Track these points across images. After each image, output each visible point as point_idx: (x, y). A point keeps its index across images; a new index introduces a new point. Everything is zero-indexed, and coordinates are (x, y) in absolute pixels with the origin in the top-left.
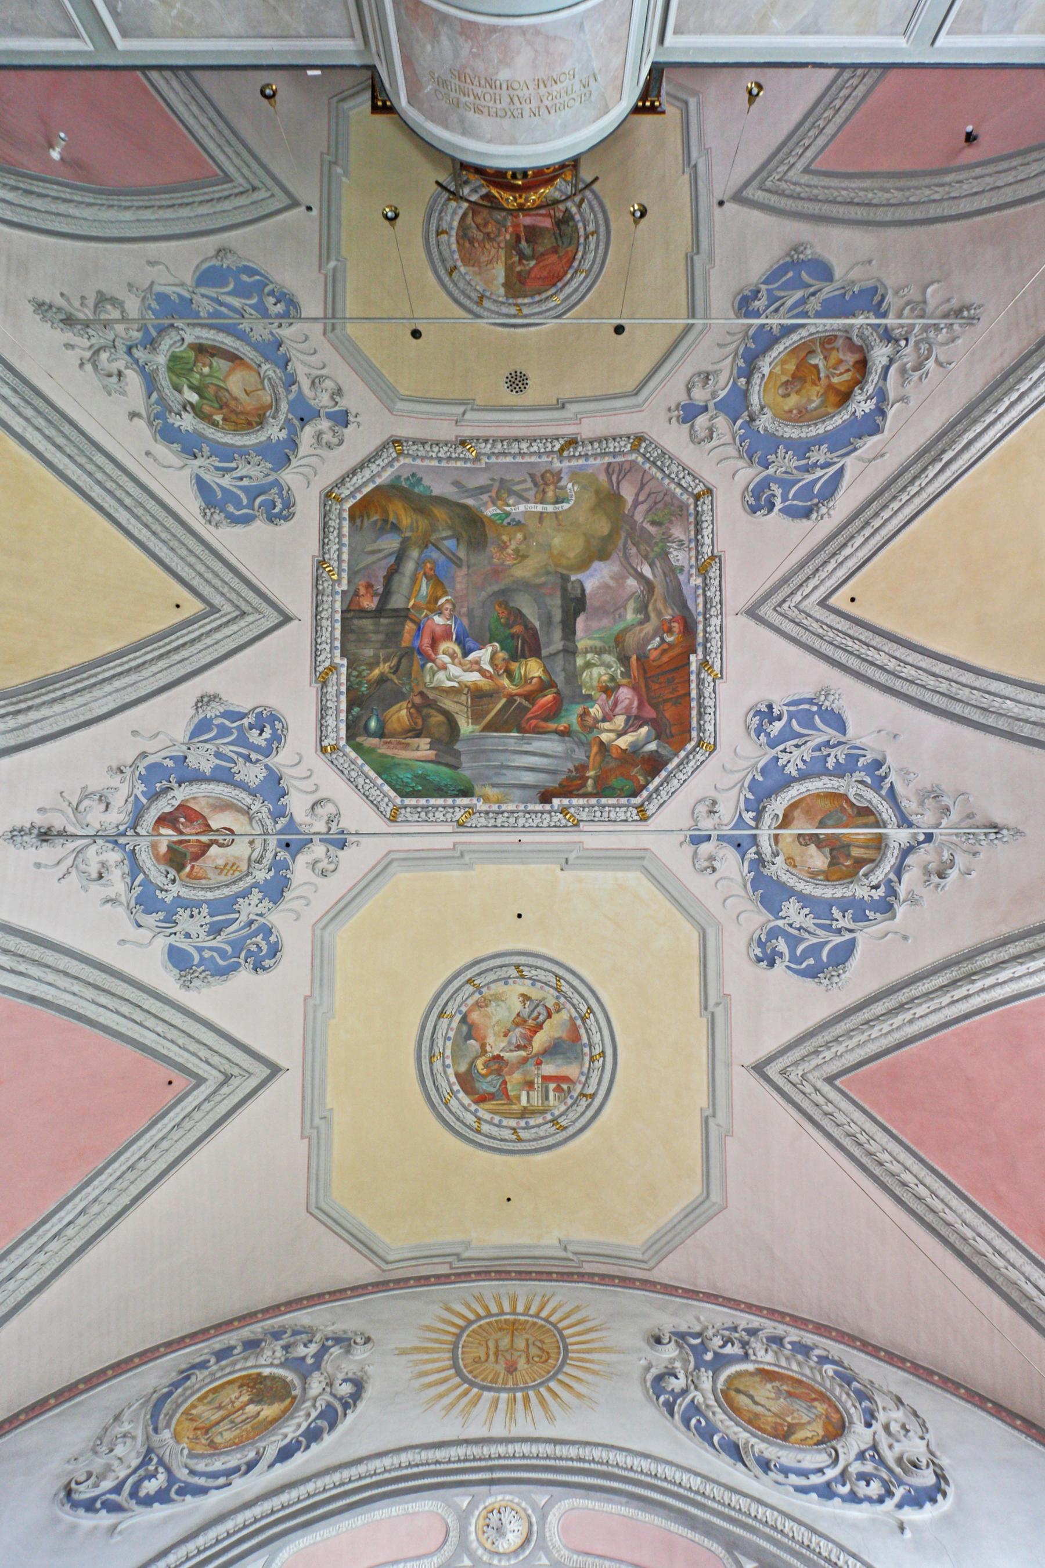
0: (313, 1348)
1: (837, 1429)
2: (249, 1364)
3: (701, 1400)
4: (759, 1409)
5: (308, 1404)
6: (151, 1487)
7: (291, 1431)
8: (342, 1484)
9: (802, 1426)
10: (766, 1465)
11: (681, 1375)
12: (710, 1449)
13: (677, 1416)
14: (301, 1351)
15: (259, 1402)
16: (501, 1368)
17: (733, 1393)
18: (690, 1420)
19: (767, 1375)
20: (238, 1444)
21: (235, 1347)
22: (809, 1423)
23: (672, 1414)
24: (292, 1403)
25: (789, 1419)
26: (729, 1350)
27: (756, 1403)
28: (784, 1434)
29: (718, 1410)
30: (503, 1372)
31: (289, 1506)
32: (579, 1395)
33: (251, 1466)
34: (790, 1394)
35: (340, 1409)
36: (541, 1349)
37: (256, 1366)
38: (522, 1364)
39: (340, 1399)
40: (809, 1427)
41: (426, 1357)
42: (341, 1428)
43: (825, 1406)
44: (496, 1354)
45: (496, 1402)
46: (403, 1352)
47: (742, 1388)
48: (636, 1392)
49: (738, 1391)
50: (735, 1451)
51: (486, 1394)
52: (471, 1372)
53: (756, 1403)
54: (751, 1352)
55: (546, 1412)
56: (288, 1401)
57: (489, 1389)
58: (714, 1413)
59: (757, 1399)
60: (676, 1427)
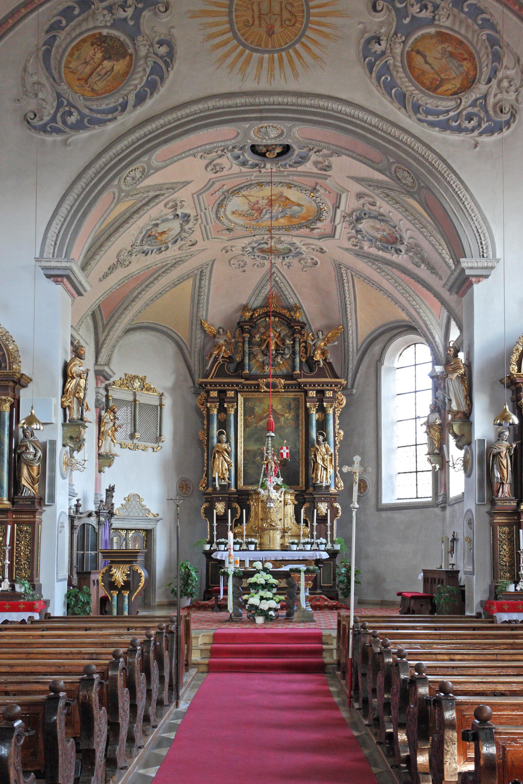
0: (130, 12)
1: (469, 84)
2: (91, 26)
3: (391, 62)
4: (427, 67)
5: (142, 62)
6: (72, 119)
7: (138, 81)
8: (179, 120)
9: (448, 80)
10: (416, 108)
11: (383, 43)
12: (388, 98)
13: (374, 75)
14: (122, 14)
15: (109, 58)
16: (263, 31)
17: (414, 54)
18: (381, 77)
19: (442, 37)
20: (110, 91)
21: (73, 8)
22: (454, 78)
23: (371, 72)
24: (131, 59)
25: (442, 76)
26: (424, 14)
27: (427, 63)
28: (433, 88)
29: (401, 70)
30: (265, 35)
31: (153, 132)
32: (315, 57)
33: (124, 107)
34: (451, 55)
35: (163, 66)
36: (290, 12)
37: (96, 28)
38: (277, 28)
39: (161, 57)
40: (453, 82)
41: (211, 20)
42: (168, 82)
43: (470, 65)
44: (260, 18)
45: (261, 61)
46: (194, 15)
47: (421, 50)
48: (351, 52)
49: (418, 52)
50: (402, 99)
51: (254, 54)
52: (243, 35)
53: (427, 63)
54: (437, 17)
55: (293, 70)
56: (128, 58)
57: (257, 51)
58: (397, 72)
59: (428, 59)
60: (371, 82)
